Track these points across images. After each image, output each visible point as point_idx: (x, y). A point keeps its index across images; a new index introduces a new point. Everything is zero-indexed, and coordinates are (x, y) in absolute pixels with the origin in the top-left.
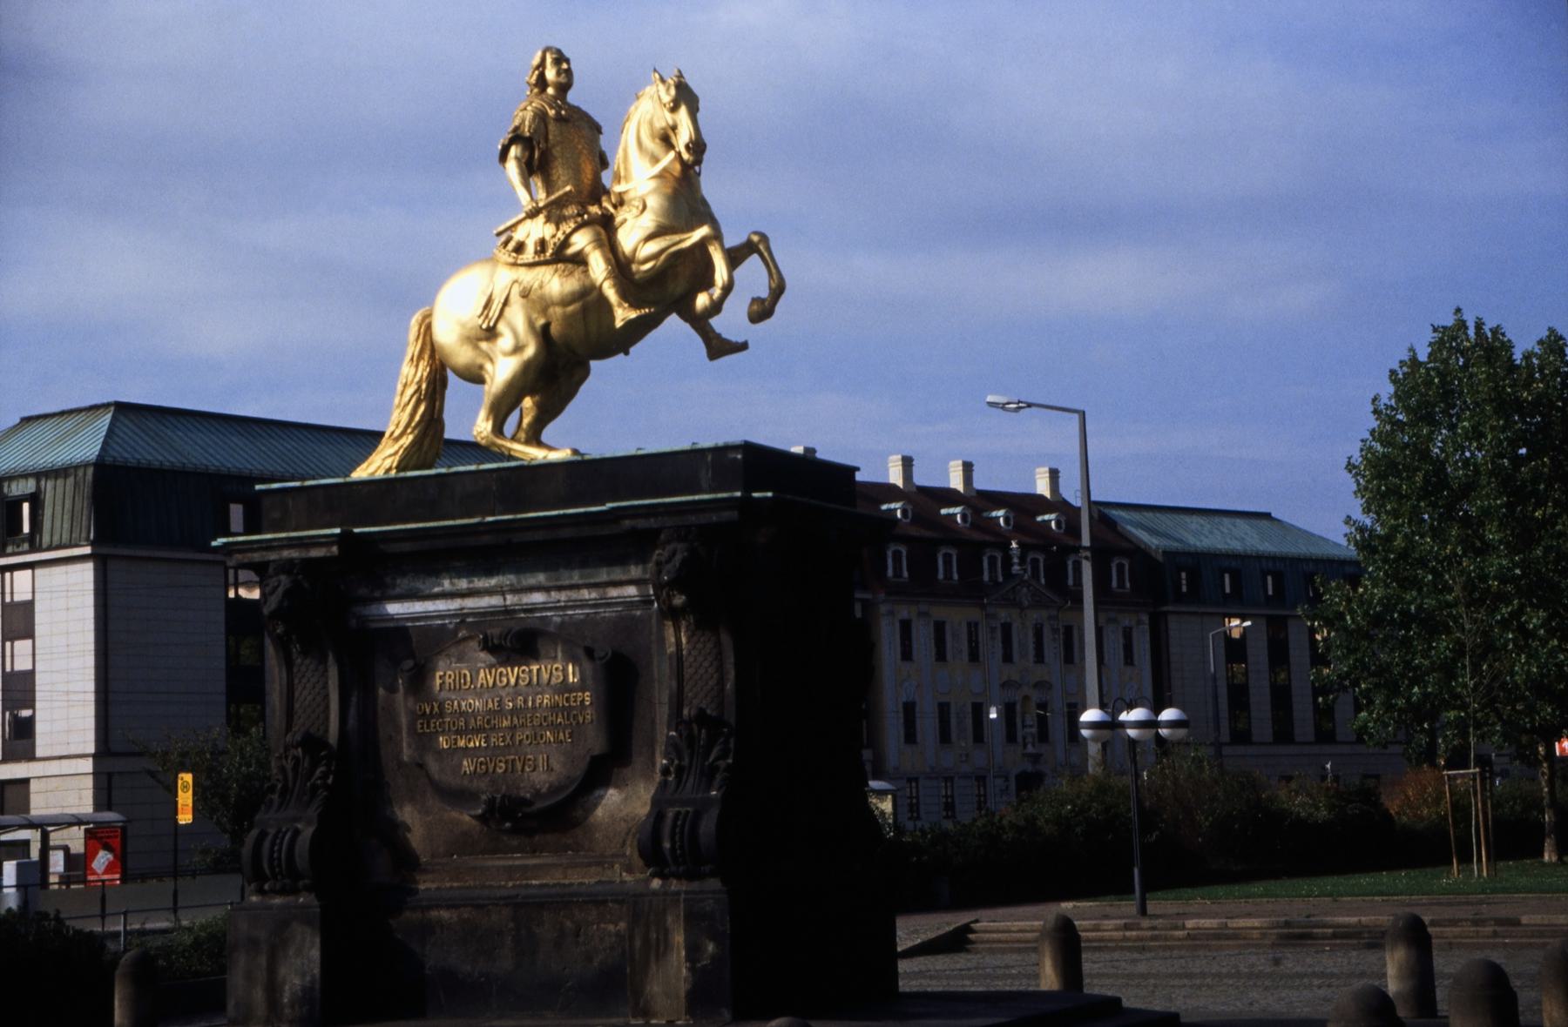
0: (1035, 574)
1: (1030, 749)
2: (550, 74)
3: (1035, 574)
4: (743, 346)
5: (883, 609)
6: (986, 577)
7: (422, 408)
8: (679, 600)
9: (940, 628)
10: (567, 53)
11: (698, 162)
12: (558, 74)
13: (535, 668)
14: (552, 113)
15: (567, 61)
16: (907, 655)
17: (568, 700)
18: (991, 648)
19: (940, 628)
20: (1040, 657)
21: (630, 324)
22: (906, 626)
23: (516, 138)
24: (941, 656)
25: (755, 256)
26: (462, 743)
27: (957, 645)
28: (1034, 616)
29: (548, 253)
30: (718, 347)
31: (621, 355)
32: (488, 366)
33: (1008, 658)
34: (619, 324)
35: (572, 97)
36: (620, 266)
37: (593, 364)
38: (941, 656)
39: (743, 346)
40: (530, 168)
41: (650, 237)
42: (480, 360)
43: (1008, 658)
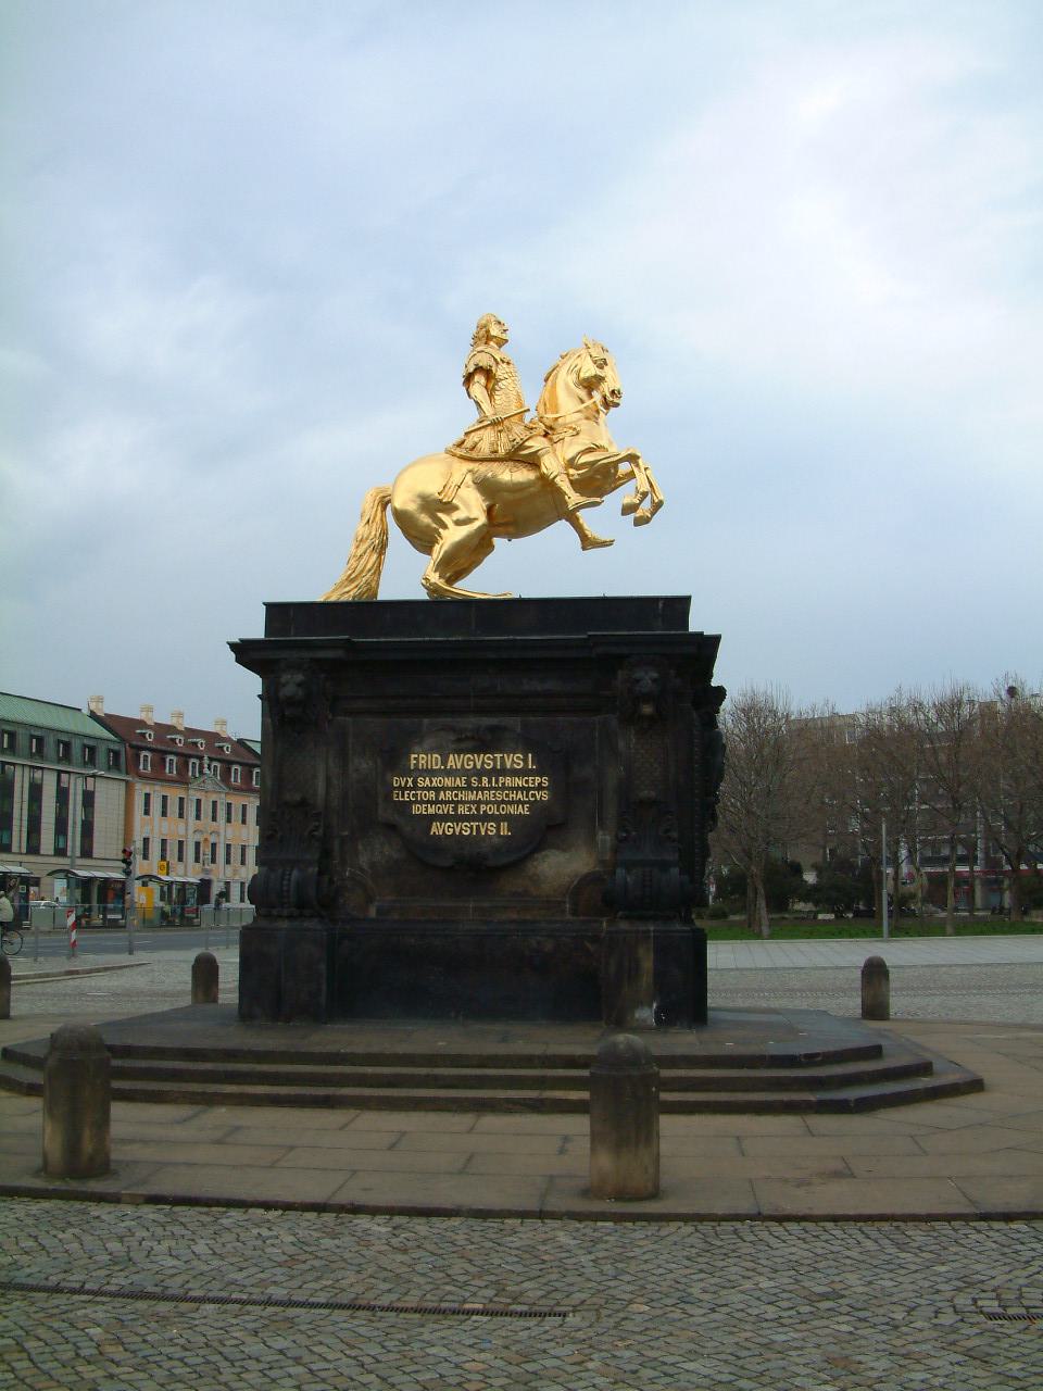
0: (215, 774)
1: (206, 867)
3: (215, 774)
4: (611, 543)
5: (138, 786)
6: (190, 774)
8: (647, 709)
9: (165, 798)
13: (498, 756)
16: (147, 812)
17: (527, 782)
18: (191, 810)
19: (165, 798)
20: (214, 819)
22: (147, 796)
24: (164, 814)
26: (431, 811)
27: (173, 808)
28: (214, 797)
29: (502, 452)
30: (587, 542)
31: (506, 540)
32: (441, 530)
33: (198, 817)
38: (164, 814)
39: (611, 543)
41: (584, 452)
42: (434, 526)
43: (198, 817)
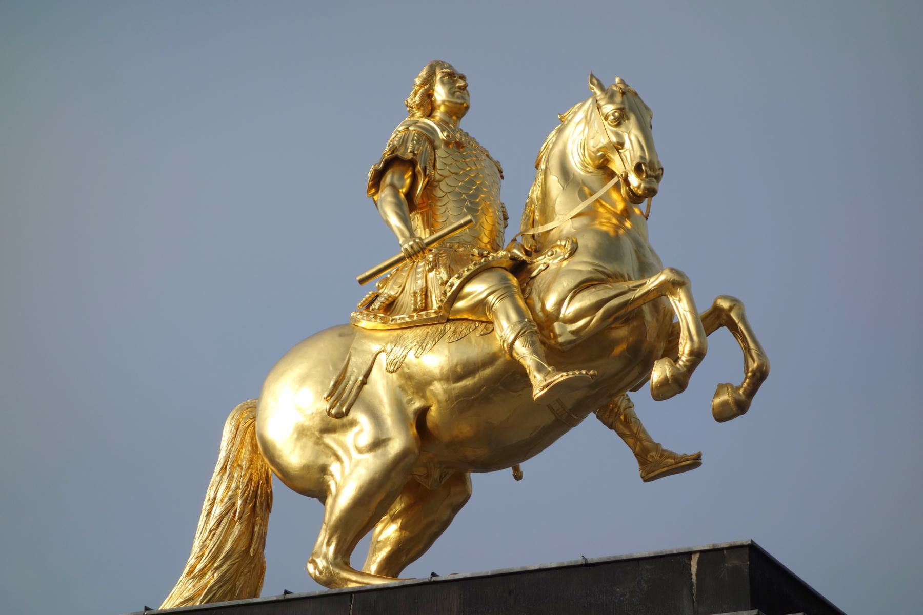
2: (440, 93)
4: (695, 462)
7: (237, 529)
10: (460, 70)
11: (651, 192)
12: (452, 93)
14: (442, 135)
15: (462, 77)
21: (554, 390)
23: (393, 161)
25: (724, 331)
32: (334, 468)
34: (538, 393)
35: (467, 124)
36: (539, 328)
37: (478, 480)
39: (695, 462)
40: (409, 203)
42: (323, 460)
